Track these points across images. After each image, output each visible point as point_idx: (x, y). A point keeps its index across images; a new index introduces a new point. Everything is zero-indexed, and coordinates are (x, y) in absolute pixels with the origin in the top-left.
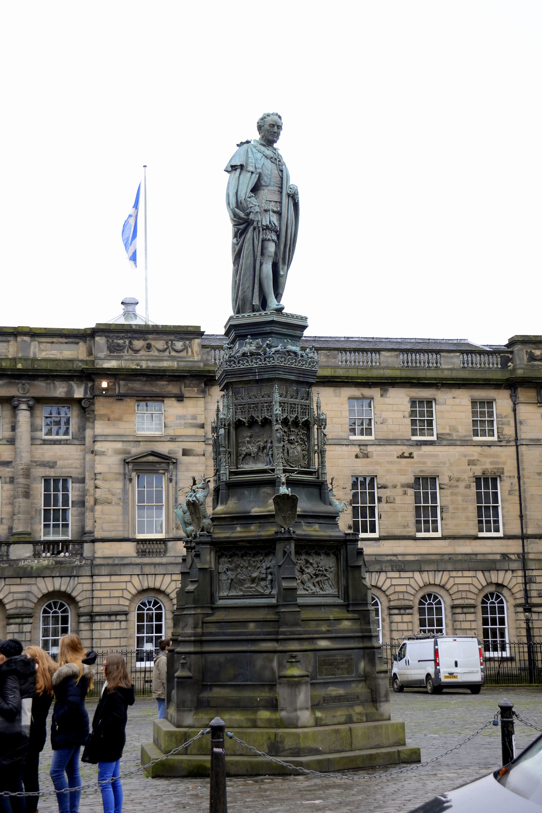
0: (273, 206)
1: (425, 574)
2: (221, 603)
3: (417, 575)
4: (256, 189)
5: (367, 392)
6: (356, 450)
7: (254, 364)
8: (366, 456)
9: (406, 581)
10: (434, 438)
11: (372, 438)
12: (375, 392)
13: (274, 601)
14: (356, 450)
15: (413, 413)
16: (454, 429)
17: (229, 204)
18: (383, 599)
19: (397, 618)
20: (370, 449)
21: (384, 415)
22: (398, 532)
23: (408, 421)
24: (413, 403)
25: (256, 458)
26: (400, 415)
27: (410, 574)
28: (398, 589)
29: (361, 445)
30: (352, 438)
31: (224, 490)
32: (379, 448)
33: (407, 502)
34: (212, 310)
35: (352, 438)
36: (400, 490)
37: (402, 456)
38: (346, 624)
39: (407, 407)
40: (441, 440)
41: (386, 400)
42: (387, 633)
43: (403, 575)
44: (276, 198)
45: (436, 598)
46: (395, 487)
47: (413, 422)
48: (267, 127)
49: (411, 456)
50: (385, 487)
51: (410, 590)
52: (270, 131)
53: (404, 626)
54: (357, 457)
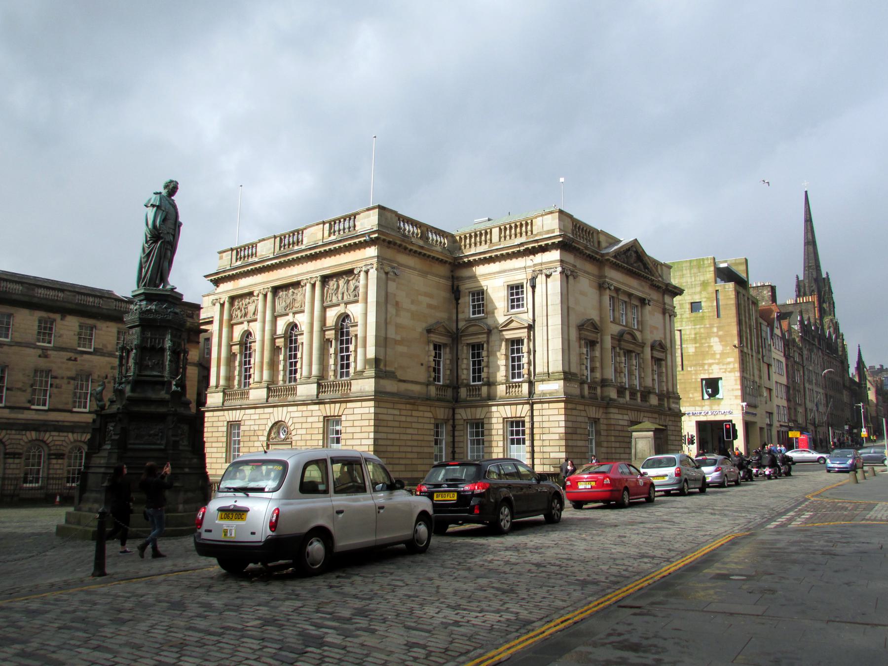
0: (171, 231)
1: (75, 435)
2: (130, 446)
3: (70, 435)
4: (164, 220)
5: (52, 316)
6: (40, 352)
7: (159, 317)
8: (46, 356)
9: (63, 438)
10: (92, 350)
11: (51, 345)
12: (57, 317)
13: (162, 447)
14: (40, 352)
15: (80, 334)
16: (105, 346)
17: (147, 224)
18: (46, 449)
19: (54, 461)
20: (49, 352)
21: (62, 332)
22: (60, 407)
23: (76, 338)
24: (81, 327)
25: (152, 369)
26: (72, 333)
27: (65, 434)
28: (57, 443)
29: (44, 349)
30: (38, 344)
31: (137, 384)
32: (55, 353)
33: (68, 387)
34: (122, 280)
35: (38, 344)
36: (65, 381)
37: (70, 359)
38: (195, 460)
39: (77, 329)
40: (96, 352)
41: (65, 323)
42: (46, 470)
43: (61, 434)
44: (173, 227)
45: (79, 449)
46: (63, 378)
47: (80, 338)
48: (171, 187)
49: (76, 360)
50: (56, 378)
51: (64, 444)
52: (172, 188)
53: (58, 466)
54: (40, 356)
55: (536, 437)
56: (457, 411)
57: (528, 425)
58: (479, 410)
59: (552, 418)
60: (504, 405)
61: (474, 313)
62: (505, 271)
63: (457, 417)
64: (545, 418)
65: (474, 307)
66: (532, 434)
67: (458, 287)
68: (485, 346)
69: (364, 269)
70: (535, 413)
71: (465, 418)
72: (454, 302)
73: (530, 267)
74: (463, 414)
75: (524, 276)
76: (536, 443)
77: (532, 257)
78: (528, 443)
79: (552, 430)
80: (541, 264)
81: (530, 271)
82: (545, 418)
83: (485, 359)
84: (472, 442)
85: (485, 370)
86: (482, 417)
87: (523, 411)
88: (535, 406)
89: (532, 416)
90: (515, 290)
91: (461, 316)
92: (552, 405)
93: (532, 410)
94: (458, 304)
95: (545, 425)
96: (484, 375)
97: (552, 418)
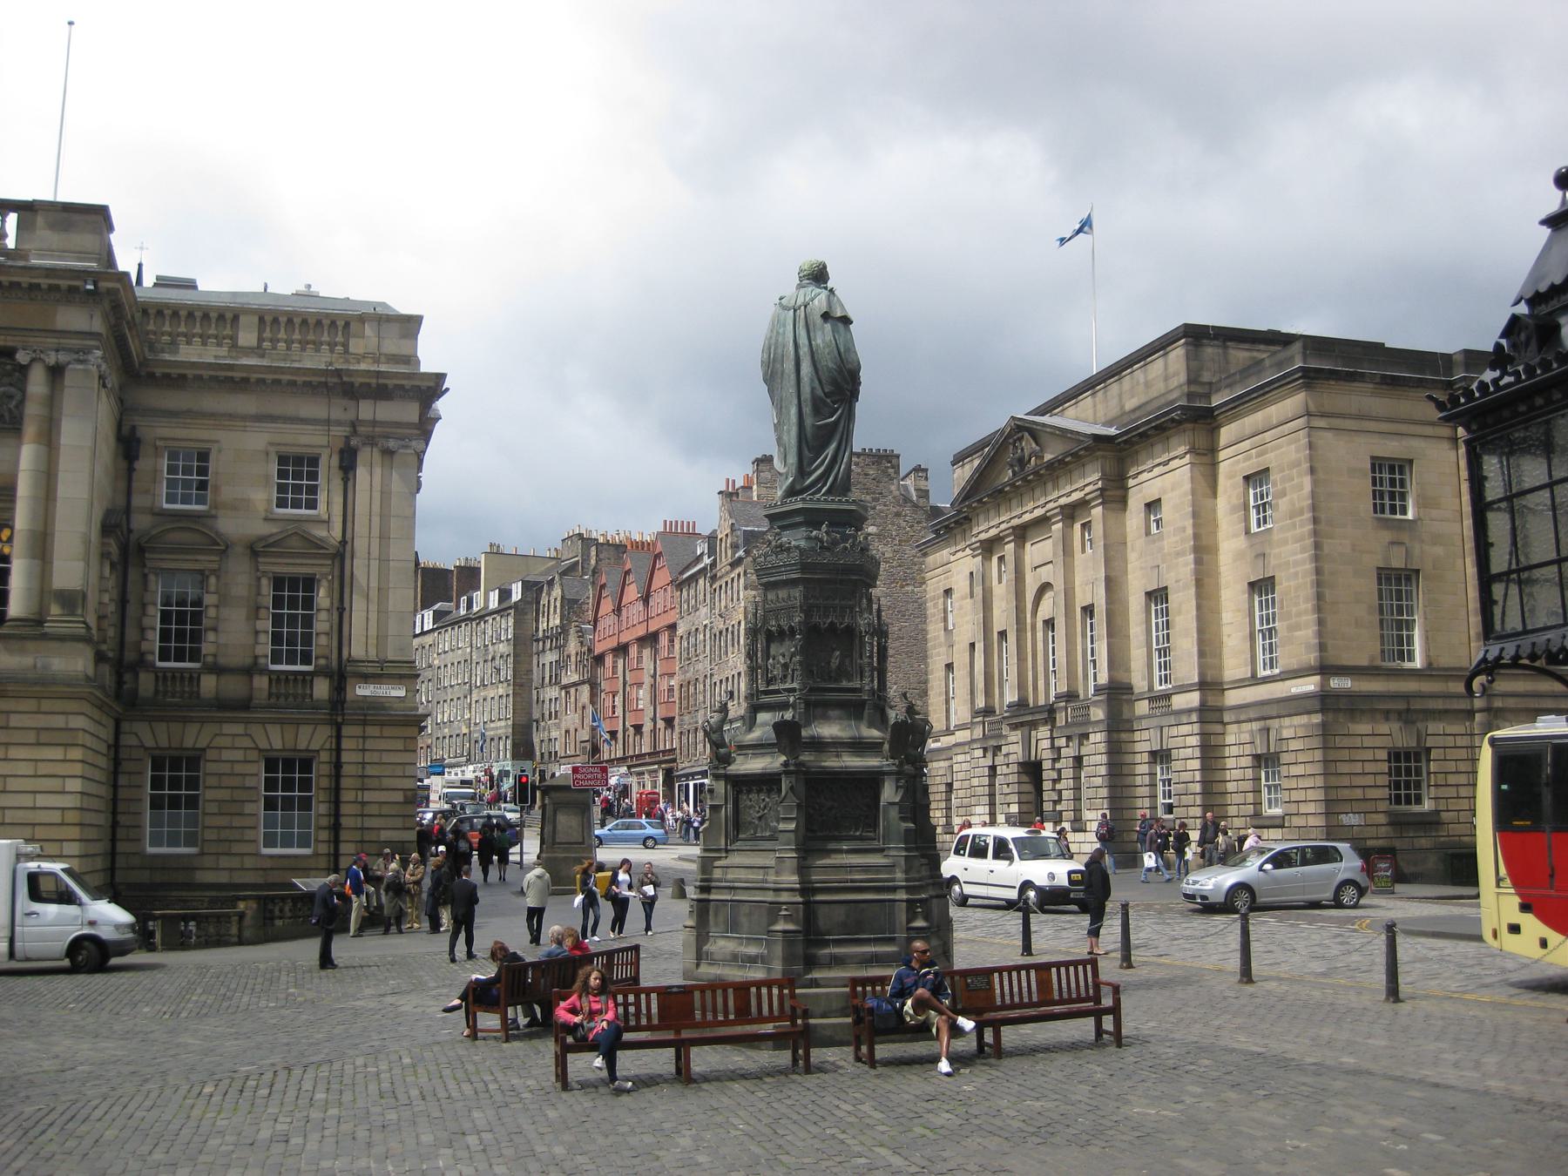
55: (346, 796)
56: (125, 726)
57: (321, 771)
58: (192, 729)
59: (386, 758)
60: (263, 722)
61: (171, 499)
62: (272, 418)
63: (127, 740)
64: (368, 757)
65: (172, 484)
66: (336, 790)
67: (133, 428)
68: (213, 580)
69: (52, 359)
70: (345, 744)
71: (150, 743)
72: (123, 464)
73: (339, 423)
74: (146, 735)
75: (323, 440)
76: (344, 809)
77: (345, 402)
78: (320, 808)
79: (386, 782)
80: (374, 423)
81: (340, 432)
82: (368, 757)
83: (212, 612)
84: (156, 804)
85: (211, 636)
86: (202, 744)
87: (314, 738)
88: (346, 731)
89: (338, 750)
90: (297, 471)
91: (137, 501)
92: (388, 731)
93: (339, 737)
94: (130, 470)
95: (370, 771)
96: (207, 648)
97: (386, 758)
